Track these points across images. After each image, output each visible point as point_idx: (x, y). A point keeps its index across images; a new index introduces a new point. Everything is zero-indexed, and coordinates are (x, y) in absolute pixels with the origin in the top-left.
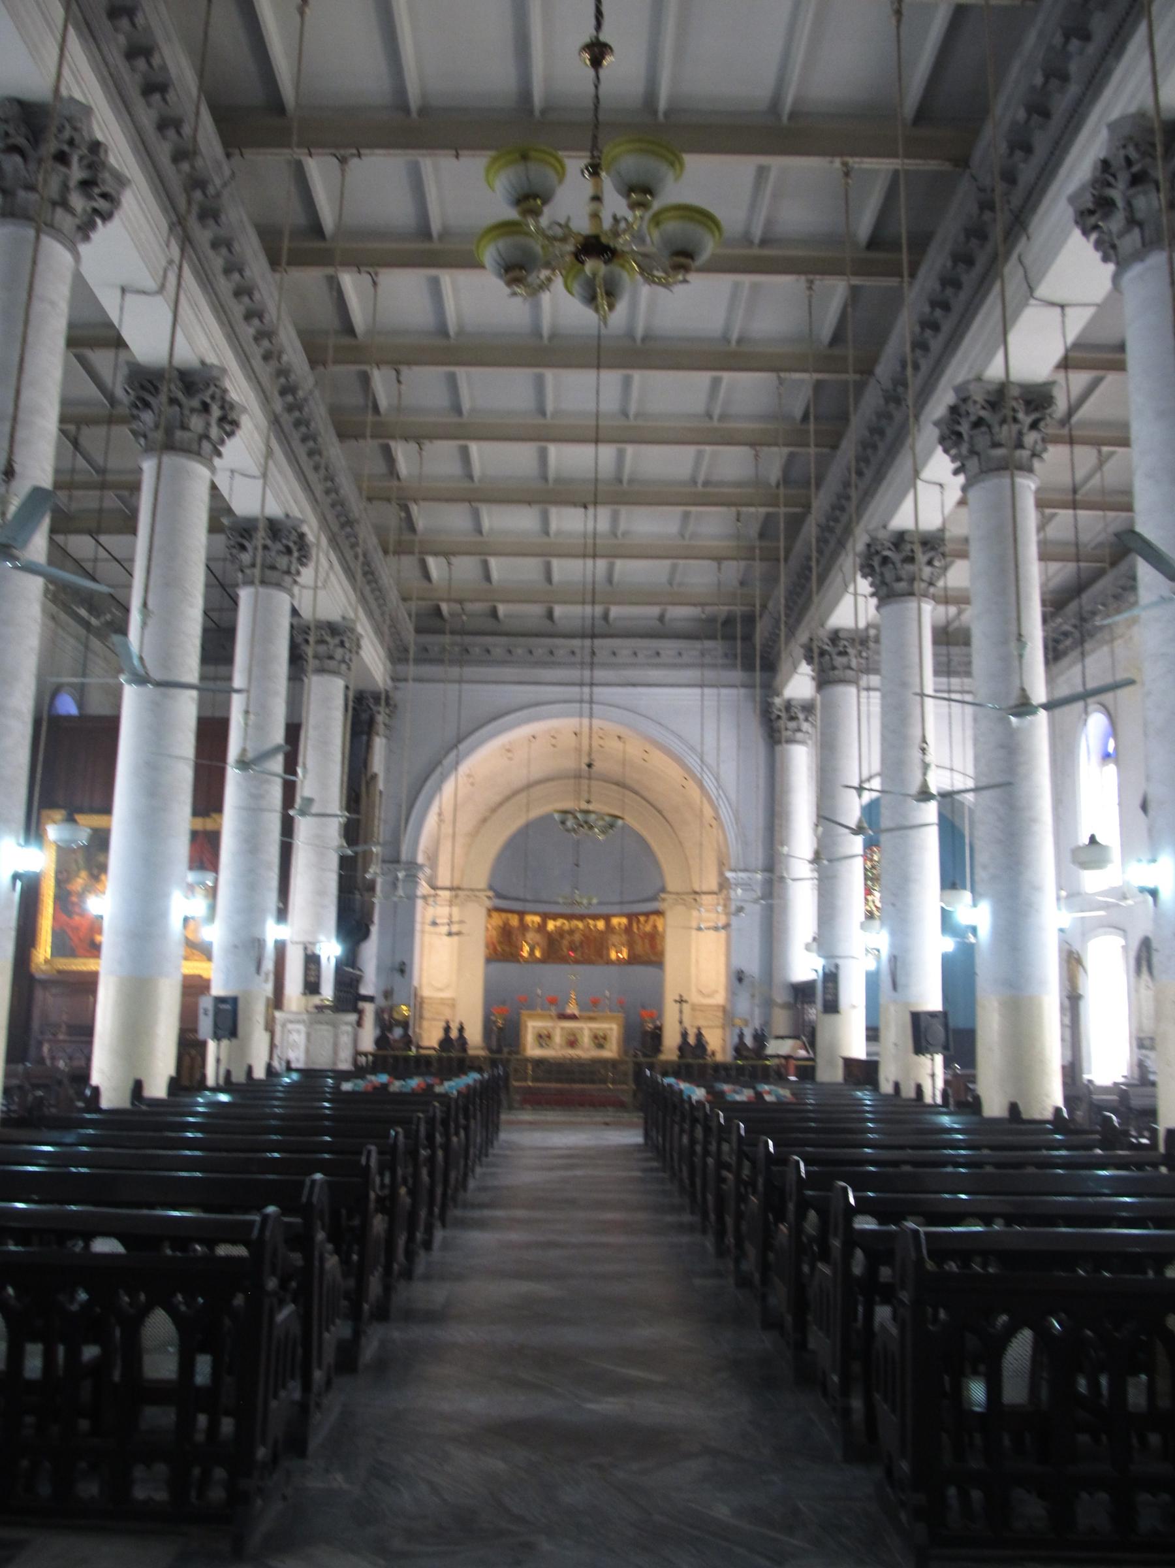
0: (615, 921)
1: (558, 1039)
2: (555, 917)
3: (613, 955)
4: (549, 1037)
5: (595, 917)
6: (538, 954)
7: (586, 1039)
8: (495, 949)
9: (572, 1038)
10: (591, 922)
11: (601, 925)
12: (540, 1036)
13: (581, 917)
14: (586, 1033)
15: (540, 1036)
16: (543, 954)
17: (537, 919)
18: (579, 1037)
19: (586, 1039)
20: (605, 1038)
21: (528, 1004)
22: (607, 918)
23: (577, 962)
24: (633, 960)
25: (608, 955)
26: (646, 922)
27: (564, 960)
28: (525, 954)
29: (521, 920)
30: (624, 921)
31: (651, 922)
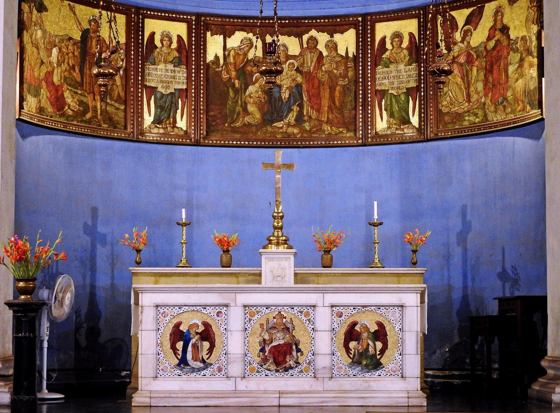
0: (384, 30)
1: (235, 342)
2: (226, 26)
3: (381, 124)
4: (207, 334)
5: (334, 25)
6: (182, 123)
7: (322, 342)
8: (59, 103)
9: (280, 339)
10: (323, 38)
11: (347, 41)
12: (178, 335)
13: (296, 26)
14: (323, 319)
15: (178, 335)
16: (194, 119)
17: (179, 29)
18: (298, 334)
19: (322, 342)
20: (380, 334)
21: (159, 258)
22: (364, 24)
23: (288, 143)
24: (440, 127)
25: (369, 121)
26: (473, 20)
27: (250, 138)
28: (148, 119)
29: (135, 29)
30: (410, 26)
31: (486, 22)
